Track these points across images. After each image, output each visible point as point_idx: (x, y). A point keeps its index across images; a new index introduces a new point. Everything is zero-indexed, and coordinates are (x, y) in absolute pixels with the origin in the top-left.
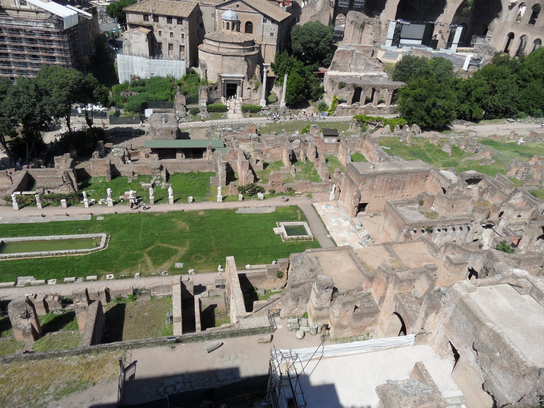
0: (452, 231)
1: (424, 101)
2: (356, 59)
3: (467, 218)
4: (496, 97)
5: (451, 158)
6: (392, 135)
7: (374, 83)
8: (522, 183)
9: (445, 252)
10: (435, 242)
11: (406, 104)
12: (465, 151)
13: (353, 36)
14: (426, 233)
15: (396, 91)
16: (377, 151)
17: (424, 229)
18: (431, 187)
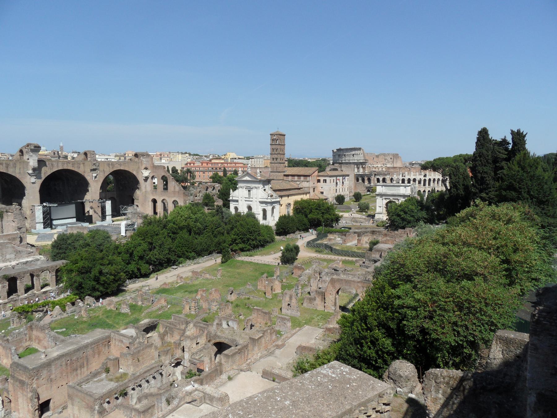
0: (146, 384)
1: (90, 272)
3: (156, 365)
4: (155, 251)
5: (132, 317)
6: (65, 315)
7: (29, 269)
8: (196, 316)
11: (73, 280)
12: (143, 305)
14: (121, 398)
15: (57, 271)
16: (50, 337)
17: (117, 395)
18: (115, 351)
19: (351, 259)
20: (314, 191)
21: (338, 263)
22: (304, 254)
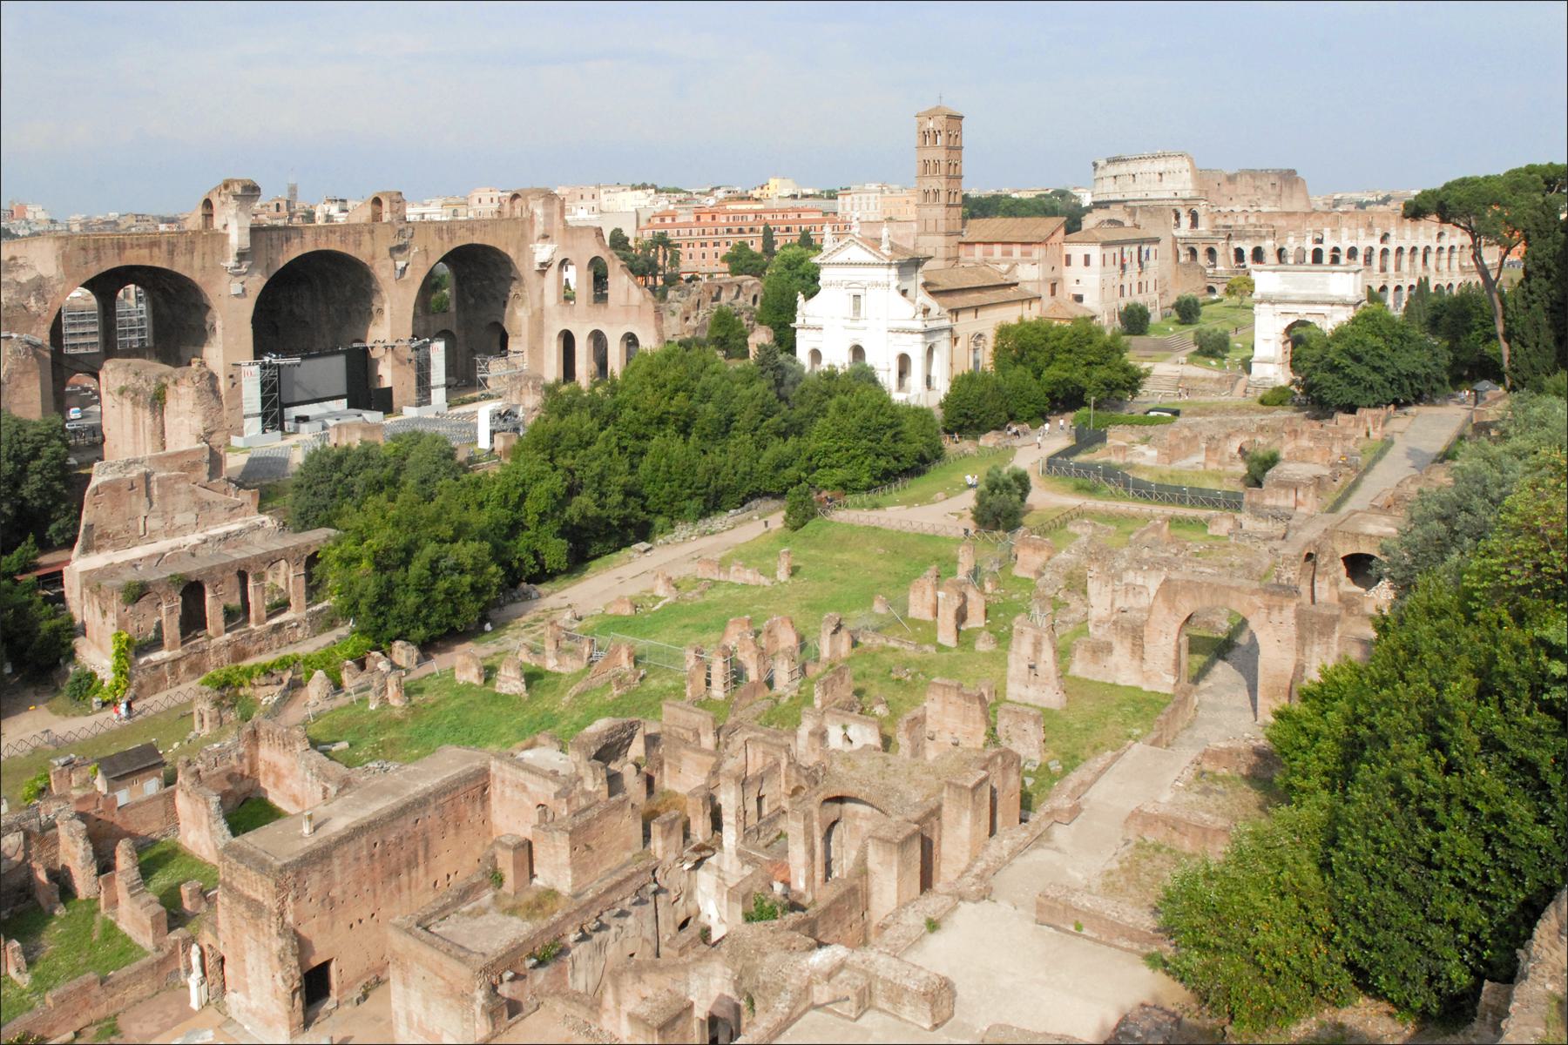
2: (162, 497)
9: (619, 1003)
10: (582, 989)
13: (135, 431)
16: (309, 767)
19: (1190, 513)
20: (1053, 294)
21: (1157, 529)
22: (1044, 498)
